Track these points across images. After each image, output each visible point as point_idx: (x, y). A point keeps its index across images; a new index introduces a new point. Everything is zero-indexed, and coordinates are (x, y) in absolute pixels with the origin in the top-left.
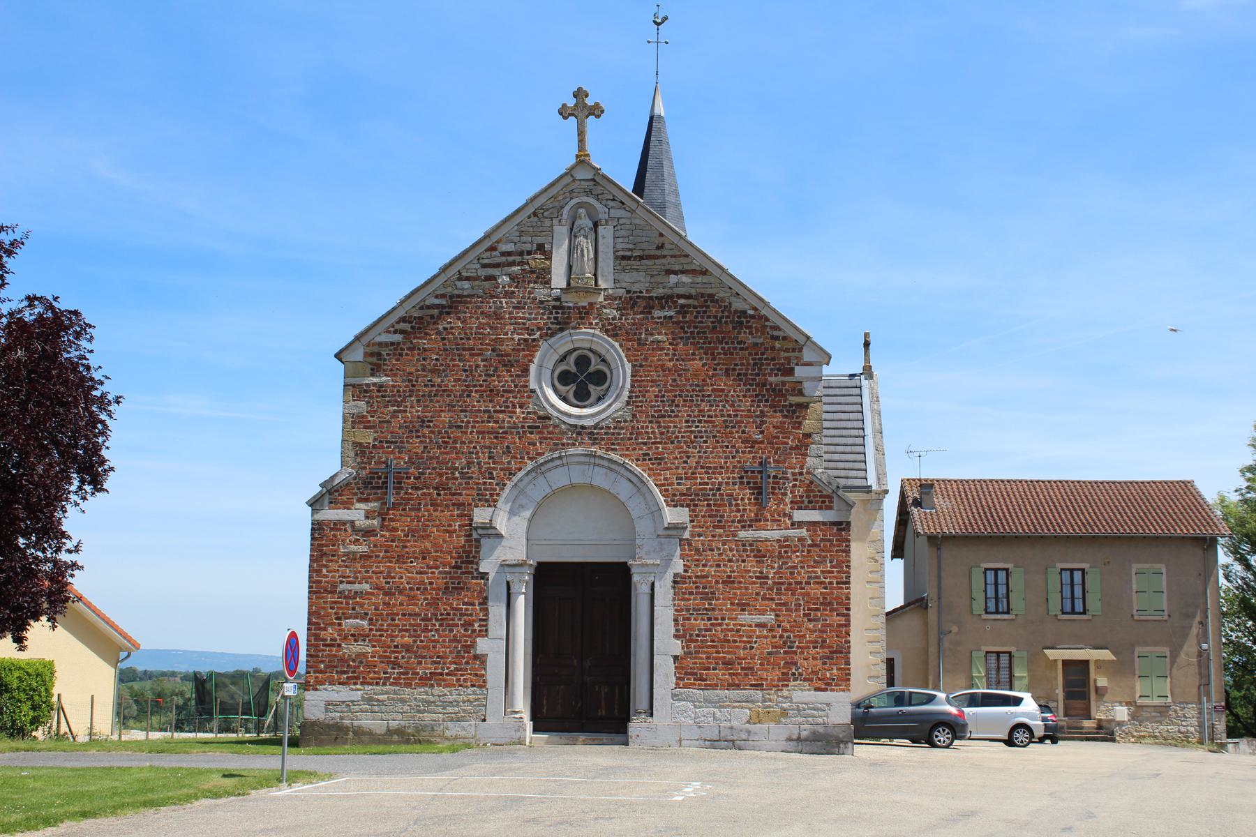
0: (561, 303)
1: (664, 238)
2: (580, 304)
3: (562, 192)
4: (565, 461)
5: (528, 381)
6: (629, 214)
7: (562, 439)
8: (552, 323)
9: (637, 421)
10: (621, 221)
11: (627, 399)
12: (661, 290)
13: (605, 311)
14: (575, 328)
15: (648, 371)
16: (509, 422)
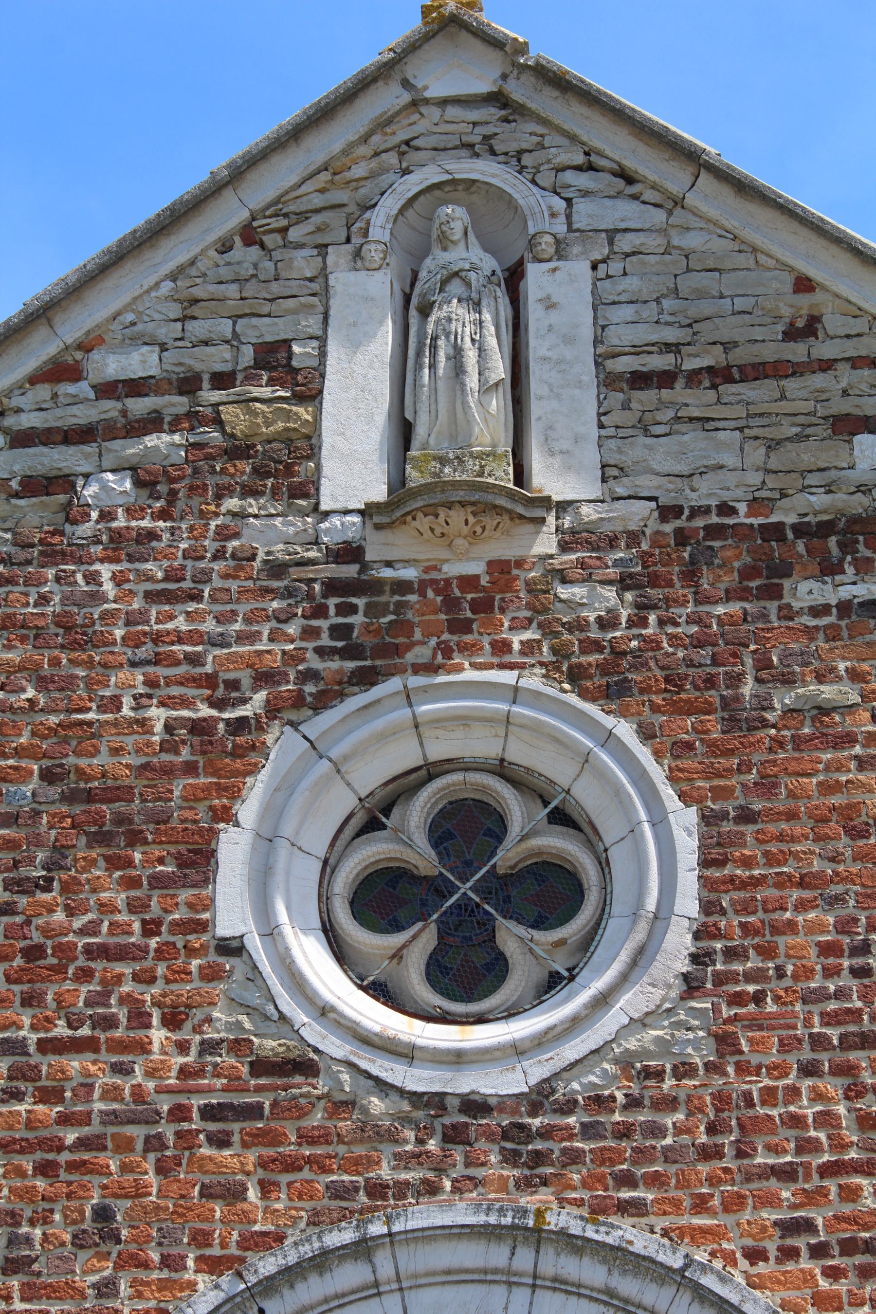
0: (365, 567)
1: (818, 296)
2: (453, 569)
3: (363, 150)
4: (385, 1269)
5: (209, 904)
6: (659, 216)
7: (373, 1163)
8: (320, 651)
9: (742, 1069)
10: (625, 243)
11: (683, 966)
12: (819, 499)
13: (563, 592)
14: (431, 668)
15: (781, 837)
16: (112, 1093)
